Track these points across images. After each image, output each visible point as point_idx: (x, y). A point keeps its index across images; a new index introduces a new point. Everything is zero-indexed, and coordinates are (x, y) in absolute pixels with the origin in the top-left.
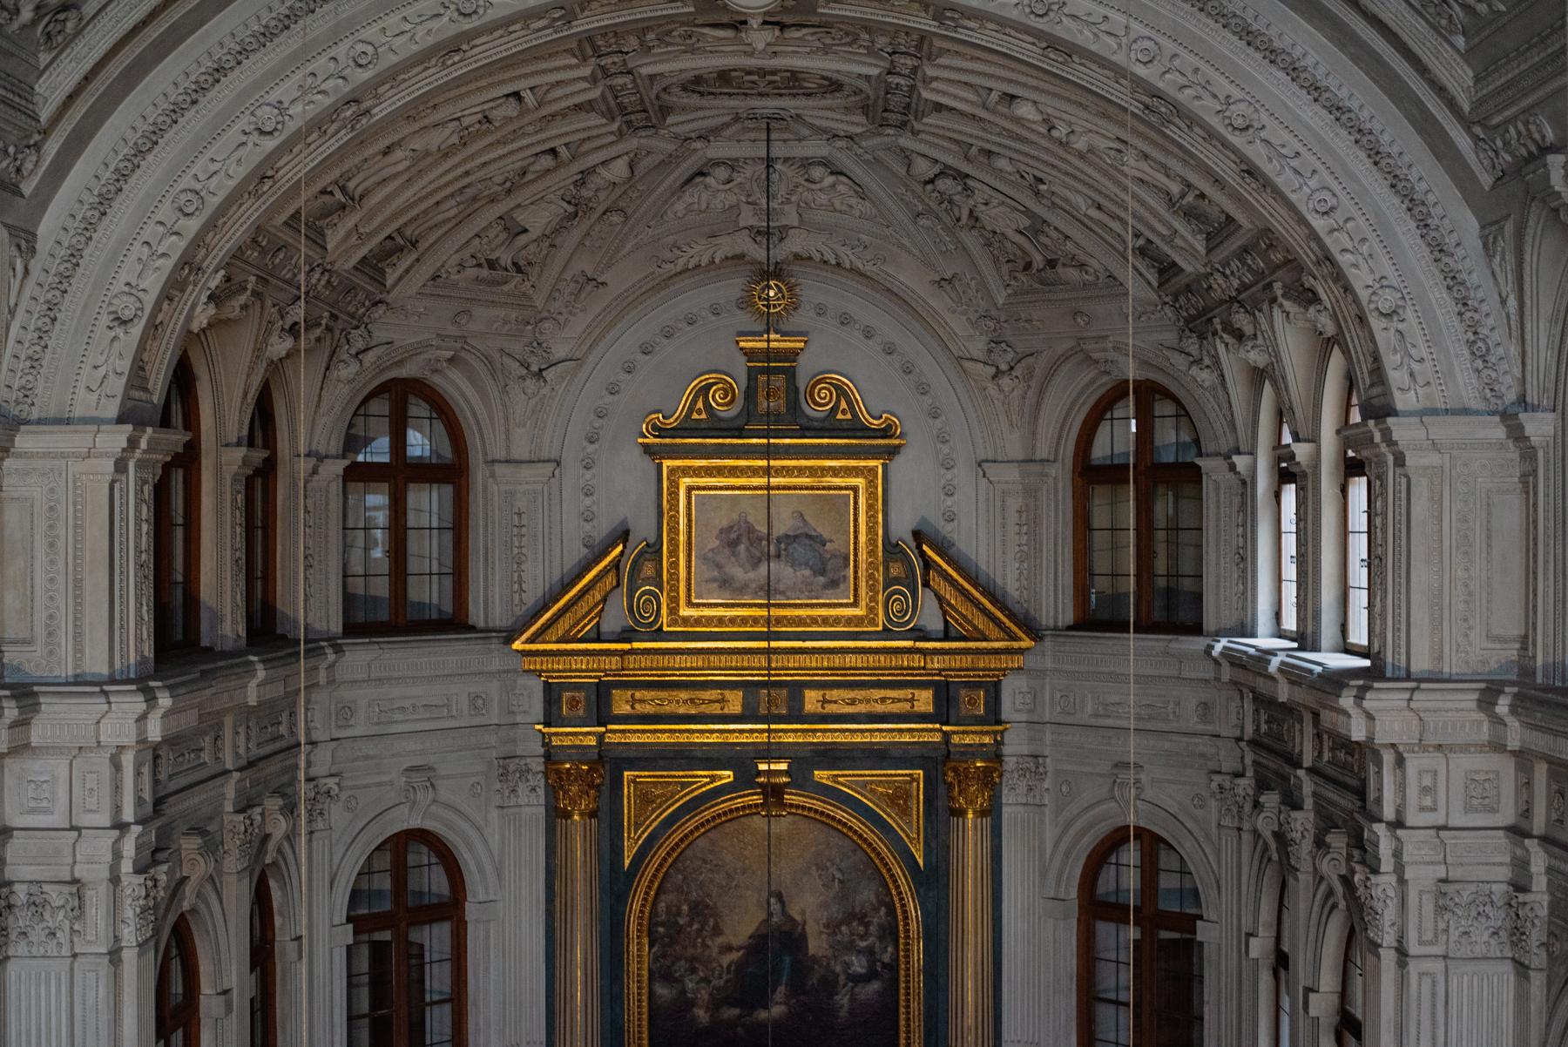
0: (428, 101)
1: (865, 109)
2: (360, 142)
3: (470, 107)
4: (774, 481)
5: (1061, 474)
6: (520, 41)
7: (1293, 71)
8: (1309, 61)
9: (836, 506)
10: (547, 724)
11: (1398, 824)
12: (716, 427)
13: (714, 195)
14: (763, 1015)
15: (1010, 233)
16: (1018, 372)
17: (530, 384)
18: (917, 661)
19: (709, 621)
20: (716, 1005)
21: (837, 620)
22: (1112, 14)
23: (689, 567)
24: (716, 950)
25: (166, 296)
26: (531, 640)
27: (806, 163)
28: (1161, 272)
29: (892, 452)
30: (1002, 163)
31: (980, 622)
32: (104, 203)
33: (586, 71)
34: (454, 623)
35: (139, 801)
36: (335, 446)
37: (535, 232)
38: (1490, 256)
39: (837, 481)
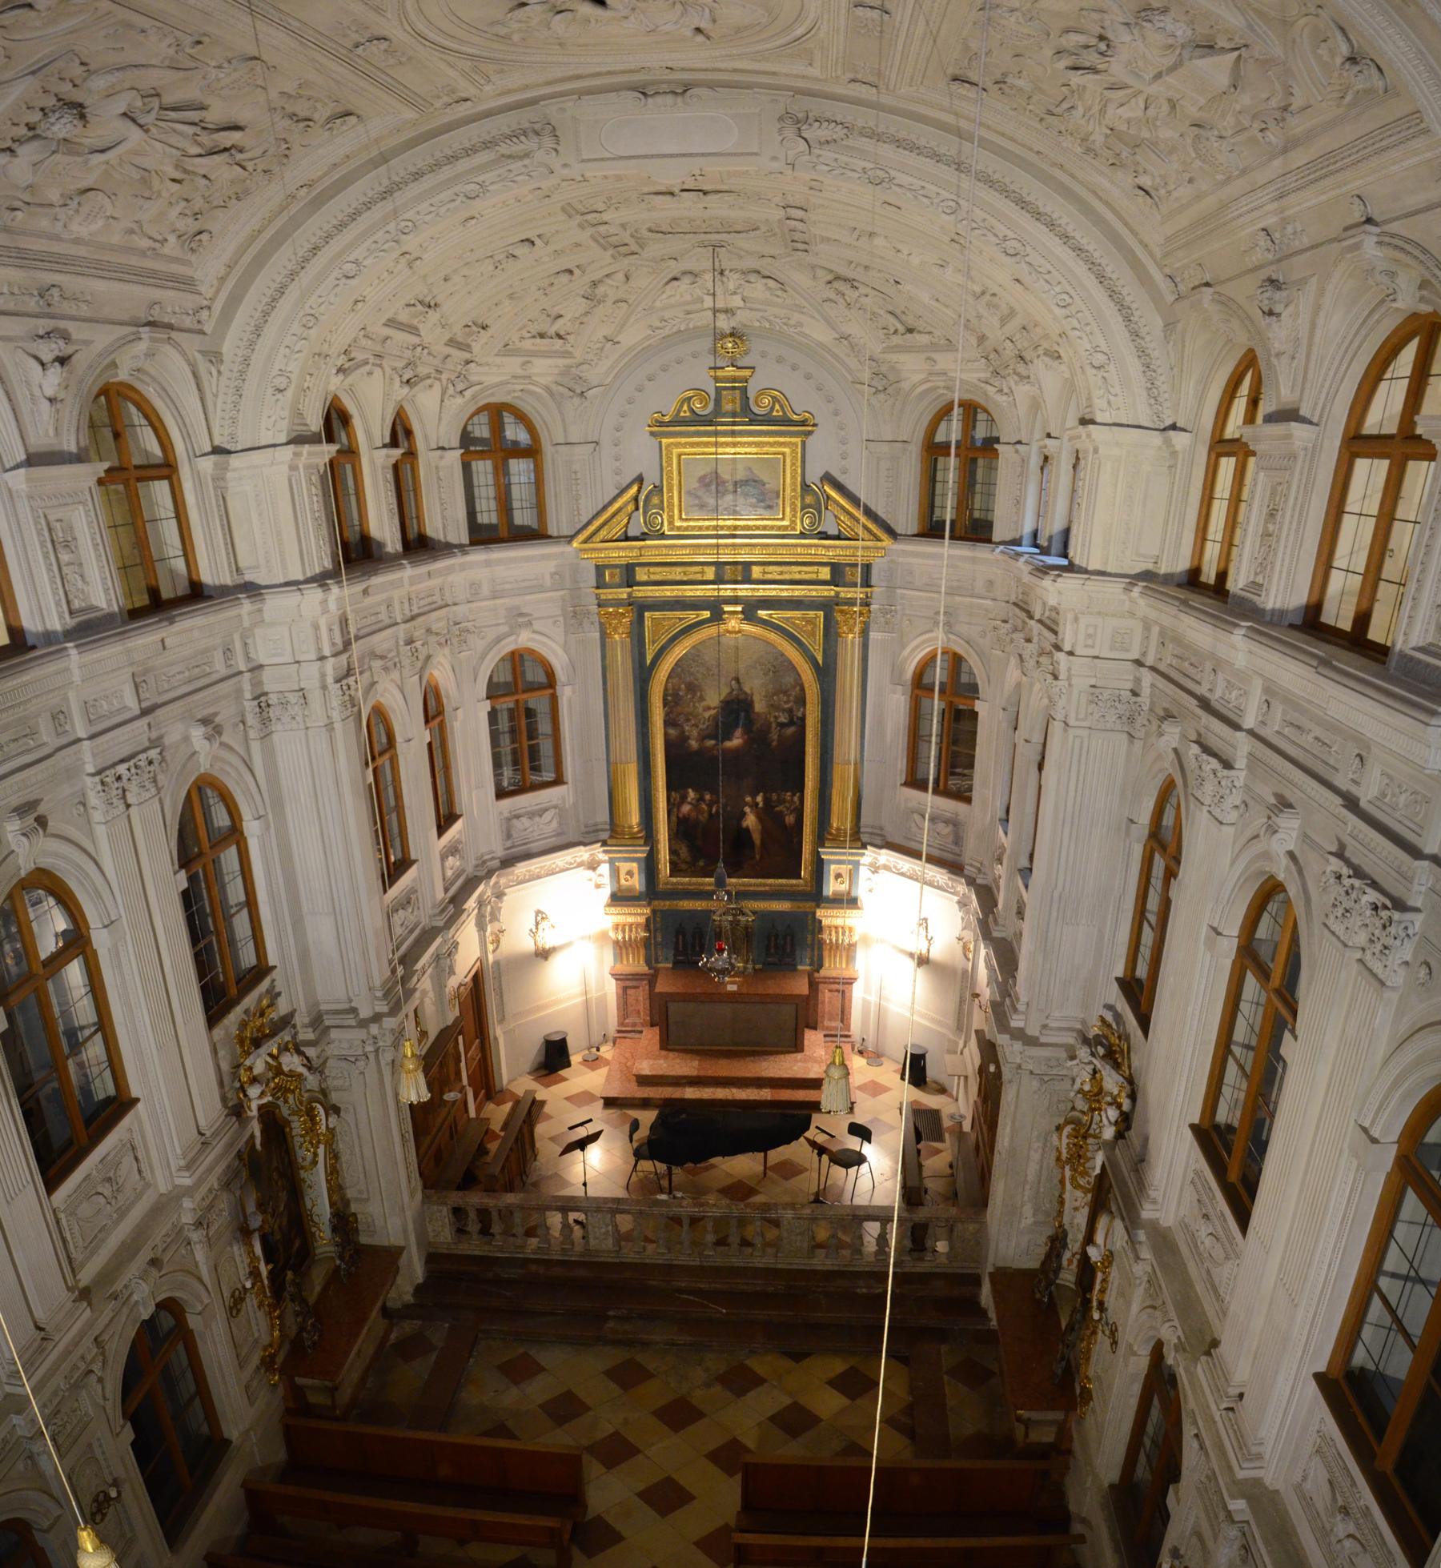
12: (697, 420)
14: (728, 744)
19: (693, 528)
20: (702, 738)
23: (680, 498)
24: (701, 710)
35: (334, 644)
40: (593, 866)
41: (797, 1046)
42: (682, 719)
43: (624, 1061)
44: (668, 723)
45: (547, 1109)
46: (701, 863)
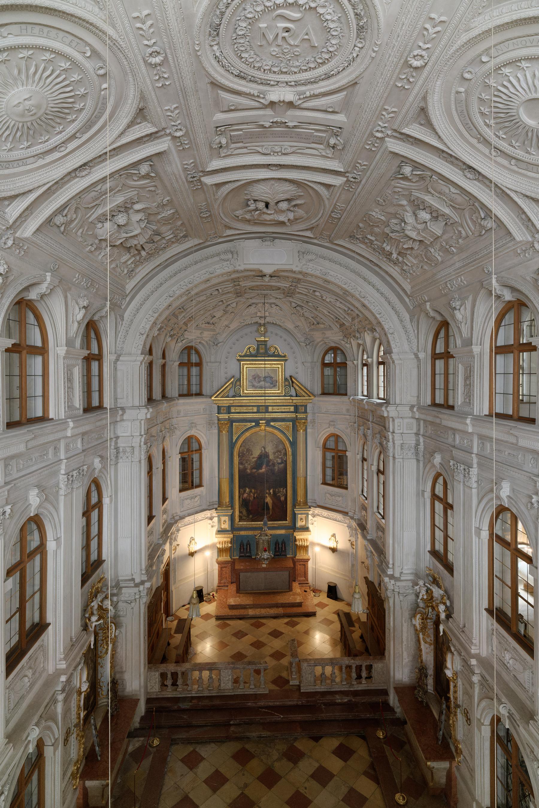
0: (202, 291)
1: (284, 293)
2: (187, 300)
3: (208, 292)
4: (266, 366)
5: (319, 364)
6: (221, 279)
7: (373, 286)
8: (377, 284)
9: (275, 371)
10: (218, 414)
11: (393, 432)
13: (252, 309)
14: (260, 471)
15: (310, 318)
16: (310, 344)
17: (215, 347)
18: (291, 401)
21: (275, 393)
22: (338, 275)
25: (150, 329)
26: (215, 397)
27: (271, 304)
28: (340, 325)
29: (286, 360)
30: (310, 304)
31: (304, 393)
32: (138, 310)
33: (232, 285)
34: (199, 394)
36: (177, 359)
37: (217, 317)
38: (411, 323)
39: (275, 366)
40: (211, 519)
41: (290, 589)
42: (244, 462)
43: (222, 599)
44: (240, 463)
45: (193, 622)
46: (251, 516)
